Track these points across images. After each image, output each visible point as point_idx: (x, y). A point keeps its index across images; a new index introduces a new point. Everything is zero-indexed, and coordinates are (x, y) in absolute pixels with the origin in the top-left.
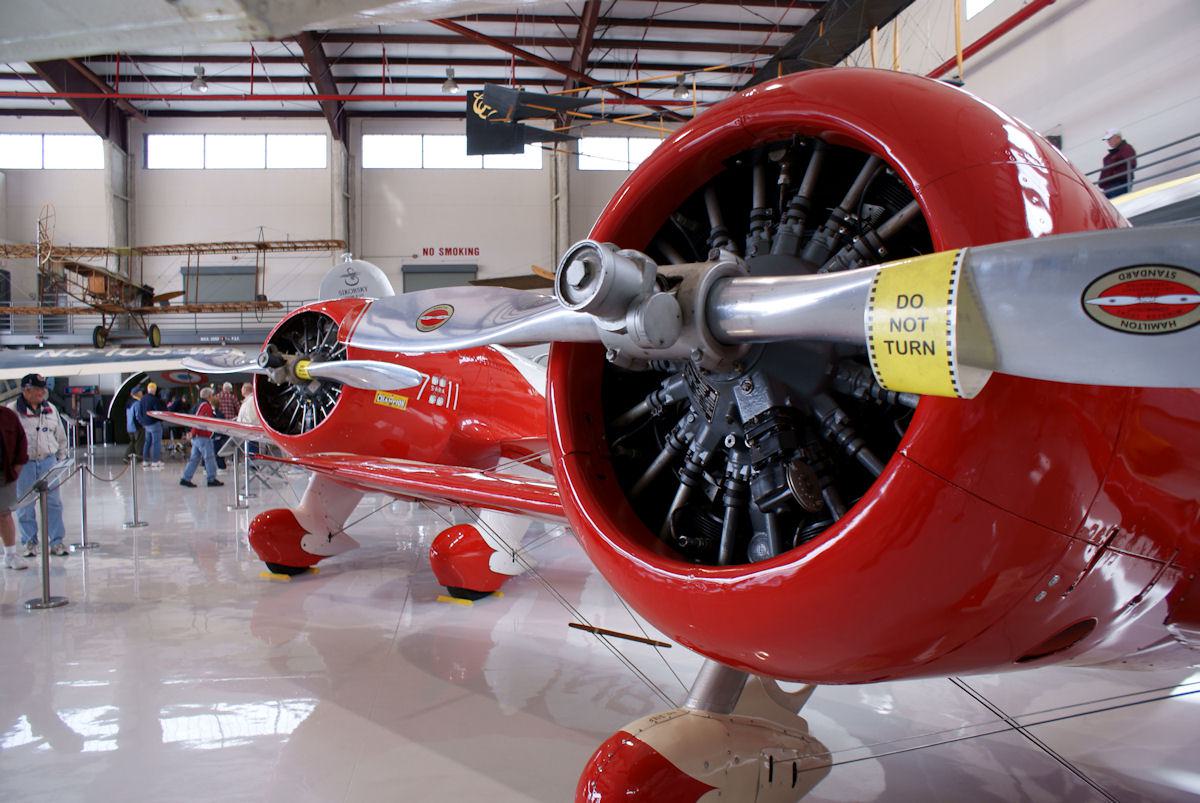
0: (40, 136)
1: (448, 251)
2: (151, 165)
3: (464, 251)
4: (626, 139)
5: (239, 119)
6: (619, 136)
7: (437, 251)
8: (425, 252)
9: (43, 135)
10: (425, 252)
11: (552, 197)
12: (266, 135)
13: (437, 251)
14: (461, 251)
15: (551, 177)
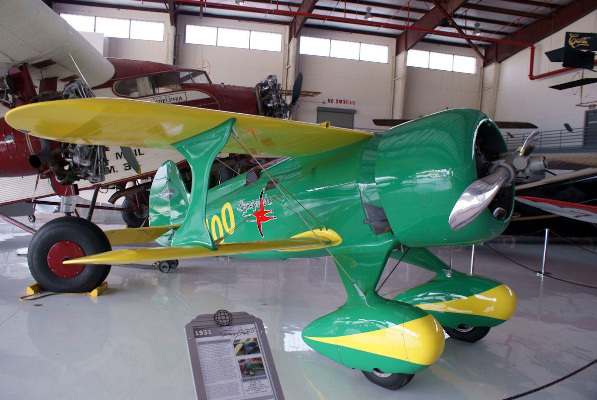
0: (129, 21)
1: (341, 101)
2: (187, 42)
3: (348, 102)
4: (452, 56)
5: (237, 21)
6: (425, 50)
7: (335, 101)
8: (329, 101)
9: (131, 20)
10: (329, 101)
11: (392, 79)
12: (250, 31)
13: (335, 101)
14: (347, 102)
15: (393, 68)
